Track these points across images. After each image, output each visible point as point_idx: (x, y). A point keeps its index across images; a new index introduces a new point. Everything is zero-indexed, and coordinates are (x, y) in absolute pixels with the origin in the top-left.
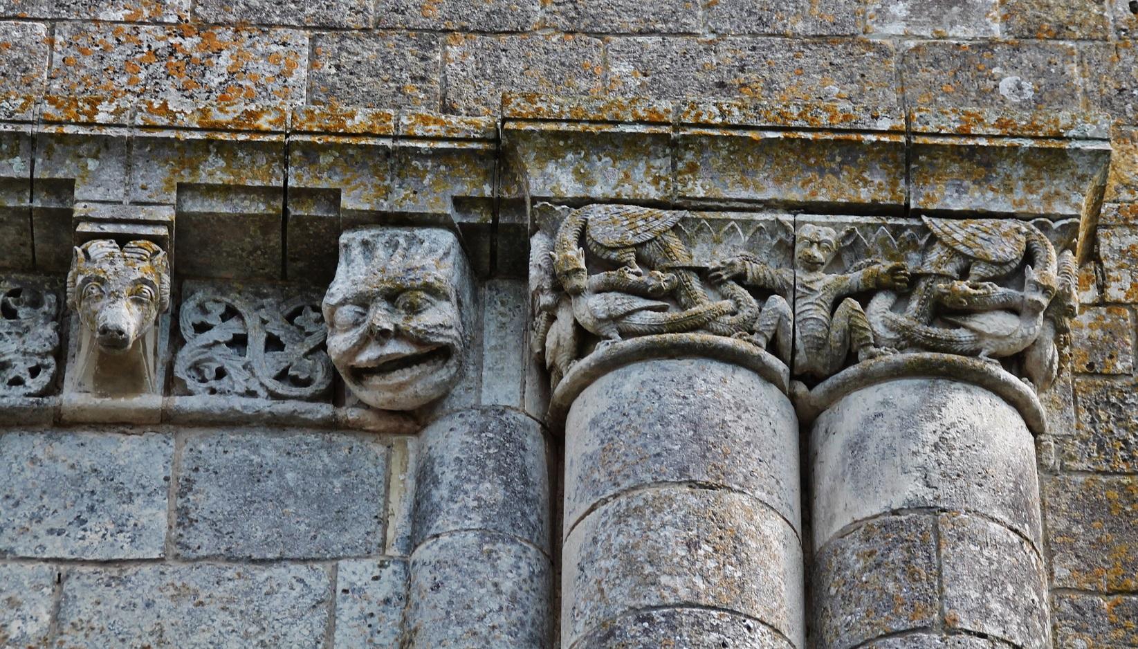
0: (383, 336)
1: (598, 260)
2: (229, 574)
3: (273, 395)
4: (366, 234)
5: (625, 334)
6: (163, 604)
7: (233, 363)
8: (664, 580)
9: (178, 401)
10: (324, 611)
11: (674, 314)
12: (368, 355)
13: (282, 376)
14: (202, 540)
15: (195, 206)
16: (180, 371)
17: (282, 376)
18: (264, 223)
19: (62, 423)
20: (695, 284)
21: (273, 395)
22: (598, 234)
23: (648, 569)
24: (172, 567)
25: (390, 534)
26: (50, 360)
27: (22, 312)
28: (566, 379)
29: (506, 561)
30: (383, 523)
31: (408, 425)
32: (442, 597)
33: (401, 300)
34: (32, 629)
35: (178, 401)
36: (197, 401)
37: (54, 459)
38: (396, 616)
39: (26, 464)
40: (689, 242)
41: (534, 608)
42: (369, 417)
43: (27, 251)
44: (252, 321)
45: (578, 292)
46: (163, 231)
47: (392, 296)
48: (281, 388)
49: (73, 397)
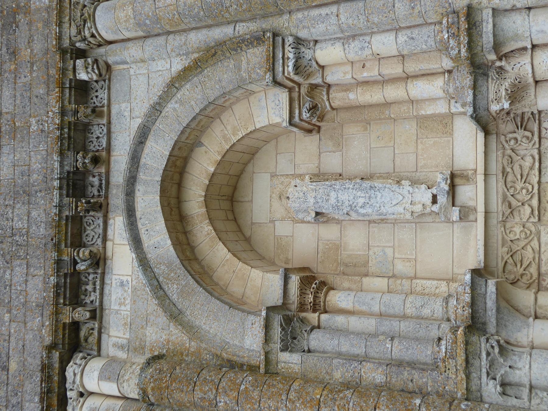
0: (93, 68)
1: (79, 33)
4: (77, 75)
6: (137, 101)
7: (100, 97)
11: (88, 20)
12: (96, 71)
13: (102, 89)
16: (101, 105)
17: (102, 89)
19: (109, 123)
20: (83, 17)
21: (105, 90)
22: (75, 34)
30: (124, 69)
33: (87, 65)
36: (106, 102)
42: (108, 73)
45: (85, 36)
47: (87, 68)
48: (104, 88)
49: (105, 121)
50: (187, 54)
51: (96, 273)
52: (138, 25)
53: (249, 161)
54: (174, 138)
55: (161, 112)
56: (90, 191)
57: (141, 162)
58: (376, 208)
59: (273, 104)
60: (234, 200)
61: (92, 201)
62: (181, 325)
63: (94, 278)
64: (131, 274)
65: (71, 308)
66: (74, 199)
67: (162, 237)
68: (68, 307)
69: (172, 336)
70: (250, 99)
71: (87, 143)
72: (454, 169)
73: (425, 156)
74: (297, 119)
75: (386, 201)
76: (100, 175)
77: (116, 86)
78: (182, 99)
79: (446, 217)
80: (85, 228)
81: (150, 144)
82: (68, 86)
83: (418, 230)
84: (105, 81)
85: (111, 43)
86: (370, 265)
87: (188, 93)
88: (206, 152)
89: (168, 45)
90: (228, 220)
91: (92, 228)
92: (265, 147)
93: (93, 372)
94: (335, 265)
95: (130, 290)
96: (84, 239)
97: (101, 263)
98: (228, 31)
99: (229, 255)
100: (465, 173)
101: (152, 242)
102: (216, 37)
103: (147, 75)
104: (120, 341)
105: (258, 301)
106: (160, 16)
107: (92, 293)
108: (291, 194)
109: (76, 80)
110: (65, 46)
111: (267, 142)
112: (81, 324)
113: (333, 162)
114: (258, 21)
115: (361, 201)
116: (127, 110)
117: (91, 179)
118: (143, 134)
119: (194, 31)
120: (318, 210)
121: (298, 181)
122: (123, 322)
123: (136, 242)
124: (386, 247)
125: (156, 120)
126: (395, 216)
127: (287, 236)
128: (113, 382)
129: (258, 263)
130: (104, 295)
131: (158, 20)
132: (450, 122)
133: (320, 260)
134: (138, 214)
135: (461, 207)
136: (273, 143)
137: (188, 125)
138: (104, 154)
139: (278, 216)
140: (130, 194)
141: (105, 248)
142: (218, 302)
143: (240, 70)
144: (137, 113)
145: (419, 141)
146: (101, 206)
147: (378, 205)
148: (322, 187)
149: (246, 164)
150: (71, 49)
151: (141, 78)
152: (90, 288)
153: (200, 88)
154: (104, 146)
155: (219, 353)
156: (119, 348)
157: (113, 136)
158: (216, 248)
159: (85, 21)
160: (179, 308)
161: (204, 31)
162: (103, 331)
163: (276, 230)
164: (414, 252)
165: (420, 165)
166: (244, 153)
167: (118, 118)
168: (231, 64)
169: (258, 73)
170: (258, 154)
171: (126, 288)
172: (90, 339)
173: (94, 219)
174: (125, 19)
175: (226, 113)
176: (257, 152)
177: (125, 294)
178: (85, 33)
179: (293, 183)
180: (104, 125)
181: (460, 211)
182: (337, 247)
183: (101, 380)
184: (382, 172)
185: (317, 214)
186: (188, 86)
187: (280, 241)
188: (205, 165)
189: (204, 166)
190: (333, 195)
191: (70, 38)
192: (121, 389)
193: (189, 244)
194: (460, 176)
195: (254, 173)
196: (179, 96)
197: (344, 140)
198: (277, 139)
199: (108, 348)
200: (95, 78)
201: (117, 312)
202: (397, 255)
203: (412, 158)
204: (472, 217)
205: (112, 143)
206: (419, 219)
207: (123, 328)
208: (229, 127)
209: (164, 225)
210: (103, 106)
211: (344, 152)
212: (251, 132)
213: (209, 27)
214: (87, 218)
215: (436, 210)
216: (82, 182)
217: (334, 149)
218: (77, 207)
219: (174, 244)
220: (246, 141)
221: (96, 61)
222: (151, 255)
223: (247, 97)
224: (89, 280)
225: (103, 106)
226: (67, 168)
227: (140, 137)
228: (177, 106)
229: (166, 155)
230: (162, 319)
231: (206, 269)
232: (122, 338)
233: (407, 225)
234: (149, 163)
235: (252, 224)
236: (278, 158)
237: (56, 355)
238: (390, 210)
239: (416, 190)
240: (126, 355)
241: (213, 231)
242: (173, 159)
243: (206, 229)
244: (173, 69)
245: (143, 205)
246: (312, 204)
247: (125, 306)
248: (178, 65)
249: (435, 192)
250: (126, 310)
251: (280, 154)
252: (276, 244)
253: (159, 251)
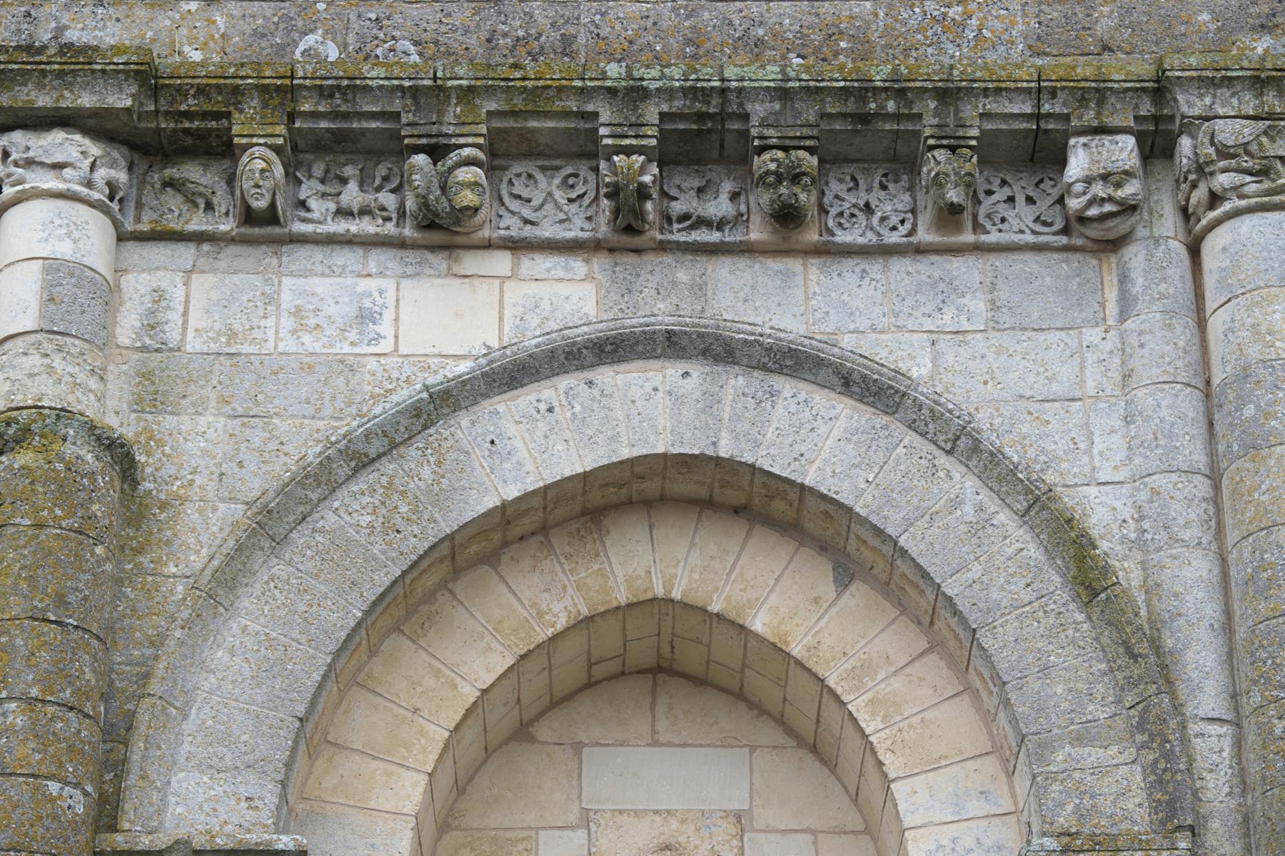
1: (1224, 153)
2: (1023, 338)
3: (1034, 232)
4: (1083, 140)
5: (1241, 197)
6: (991, 356)
7: (1010, 214)
8: (1278, 344)
9: (984, 238)
10: (1077, 359)
11: (1267, 185)
12: (1093, 212)
13: (1037, 220)
14: (1006, 318)
15: (989, 126)
16: (981, 219)
17: (1037, 220)
18: (1027, 132)
19: (920, 250)
21: (1034, 232)
22: (1220, 137)
23: (1268, 338)
24: (992, 334)
25: (1108, 312)
26: (909, 215)
27: (891, 186)
28: (1204, 222)
29: (1179, 330)
30: (1103, 305)
31: (1110, 246)
32: (1145, 352)
34: (924, 372)
35: (984, 238)
36: (993, 237)
37: (918, 272)
38: (1117, 361)
39: (904, 276)
40: (1272, 140)
41: (1195, 355)
42: (1089, 244)
43: (892, 152)
44: (1017, 188)
45: (1212, 174)
46: (974, 143)
47: (1105, 177)
48: (1038, 228)
49: (925, 235)
50: (1140, 543)
51: (402, 214)
52: (1245, 374)
53: (791, 732)
54: (861, 502)
55: (949, 452)
56: (685, 185)
57: (781, 379)
59: (969, 842)
60: (661, 677)
61: (649, 206)
62: (239, 548)
63: (383, 209)
64: (403, 350)
65: (280, 141)
66: (653, 142)
67: (530, 466)
68: (281, 129)
69: (201, 511)
70: (991, 759)
71: (850, 169)
76: (740, 220)
77: (1046, 277)
78: (990, 530)
80: (558, 168)
81: (839, 417)
82: (1046, 108)
84: (1065, 231)
85: (1195, 251)
87: (1010, 551)
88: (816, 600)
89: (1174, 477)
90: (590, 665)
91: (559, 195)
92: (838, 788)
93: (69, 235)
95: (347, 349)
96: (517, 168)
97: (436, 237)
98: (1205, 693)
99: (469, 694)
101: (512, 429)
102: (1190, 655)
103: (1078, 394)
104: (175, 317)
105: (319, 799)
106: (1264, 458)
107: (332, 206)
109: (1067, 135)
110: (1180, 98)
111: (856, 797)
112: (227, 163)
114: (1233, 803)
116: (963, 318)
117: (728, 186)
118: (874, 389)
119: (1216, 571)
122: (237, 326)
123: (510, 374)
125: (923, 435)
128: (42, 316)
129: (445, 781)
130: (327, 249)
131: (1254, 447)
134: (606, 375)
137: (904, 553)
138: (812, 236)
140: (670, 345)
141: (488, 246)
142: (317, 677)
143: (1078, 740)
144: (949, 359)
146: (629, 230)
149: (780, 721)
150: (1172, 117)
151: (1067, 372)
152: (352, 195)
153: (1026, 596)
154: (842, 237)
155: (155, 687)
156: (152, 312)
157: (875, 267)
158: (495, 645)
159: (1263, 173)
160: (294, 535)
161: (1212, 611)
162: (206, 247)
163: (556, 833)
166: (818, 722)
167: (934, 285)
168: (1099, 712)
169: (1062, 805)
170: (817, 764)
171: (353, 335)
172: (174, 201)
173: (587, 201)
174: (1263, 329)
175: (946, 672)
176: (824, 762)
177: (332, 331)
178: (1224, 171)
180: (912, 232)
183: (47, 271)
186: (1034, 552)
187: (521, 847)
188: (773, 600)
189: (770, 596)
191: (1208, 119)
192: (19, 344)
193: (506, 544)
195: (753, 749)
196: (1003, 517)
198: (867, 830)
199: (149, 271)
200: (1074, 204)
201: (271, 300)
205: (849, 263)
207: (217, 326)
208: (897, 683)
209: (568, 473)
210: (977, 227)
212: (881, 764)
213: (1228, 628)
214: (592, 177)
216: (716, 153)
218: (628, 151)
219: (505, 506)
220: (851, 744)
221: (1129, 208)
222: (465, 428)
223: (996, 749)
224: (378, 190)
225: (977, 227)
226: (758, 110)
227: (864, 378)
228: (968, 510)
229: (805, 474)
230: (257, 480)
231: (424, 609)
232: (185, 328)
234: (779, 407)
235: (578, 747)
237: (121, 99)
240: (127, 342)
241: (550, 632)
242: (793, 495)
243: (557, 607)
244: (1093, 491)
245: (635, 392)
247: (294, 332)
248: (1104, 513)
250: (277, 336)
251: (815, 843)
252: (508, 835)
253: (480, 458)
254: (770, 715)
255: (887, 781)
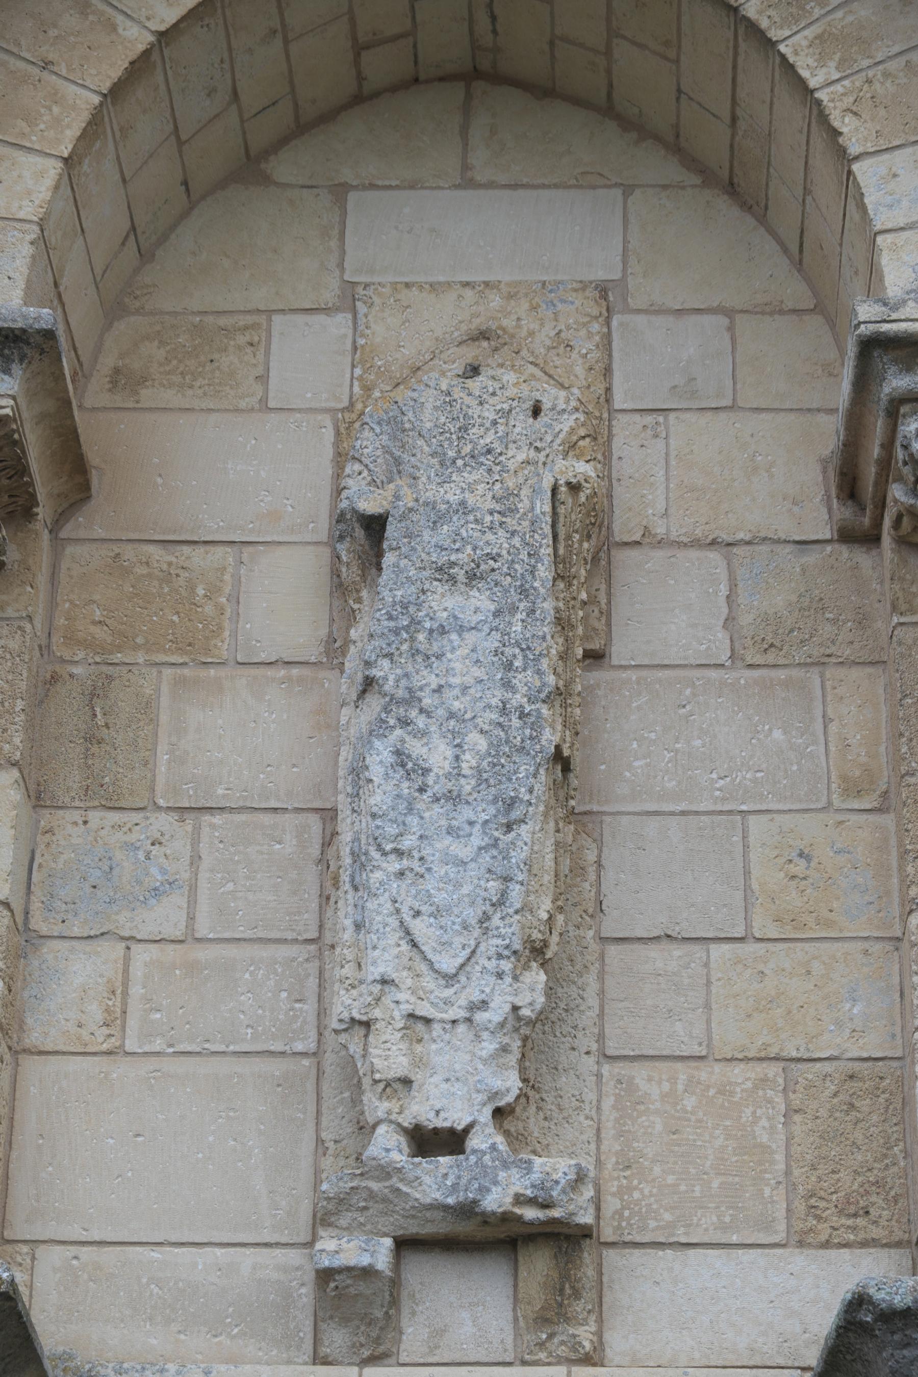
58: (392, 830)
60: (479, 86)
72: (610, 1255)
73: (690, 1102)
74: (897, 382)
75: (430, 884)
79: (342, 1202)
83: (276, 1067)
86: (95, 817)
90: (359, 49)
92: (771, 246)
94: (100, 633)
100: (579, 1307)
108: (492, 386)
113: (671, 612)
115: (437, 755)
120: (392, 530)
121: (567, 423)
124: (192, 902)
126: (348, 935)
127: (263, 379)
132: (876, 1232)
133: (129, 552)
135: (395, 1283)
136: (795, 292)
139: (381, 327)
145: (773, 1070)
147: (407, 843)
148: (524, 544)
149: (676, 146)
163: (300, 319)
164: (158, 1045)
165: (640, 1073)
166: (734, 119)
170: (736, 212)
176: (746, 207)
179: (550, 396)
181: (367, 1273)
182: (198, 644)
184: (609, 876)
185: (375, 526)
187: (242, 339)
190: (478, 603)
194: (565, 1276)
195: (628, 190)
197: (795, 673)
198: (818, 309)
202: (142, 955)
203: (682, 1036)
204: (337, 1339)
206: (334, 1064)
211: (729, 676)
212: (836, 133)
215: (374, 1150)
217: (746, 620)
220: (790, 115)
233: (309, 1008)
235: (340, 192)
236: (706, 319)
238: (379, 909)
239: (489, 1046)
246: (431, 492)
249: (475, 1142)
251: (731, 328)
252: (223, 321)
254: (658, 138)
255: (844, 159)
